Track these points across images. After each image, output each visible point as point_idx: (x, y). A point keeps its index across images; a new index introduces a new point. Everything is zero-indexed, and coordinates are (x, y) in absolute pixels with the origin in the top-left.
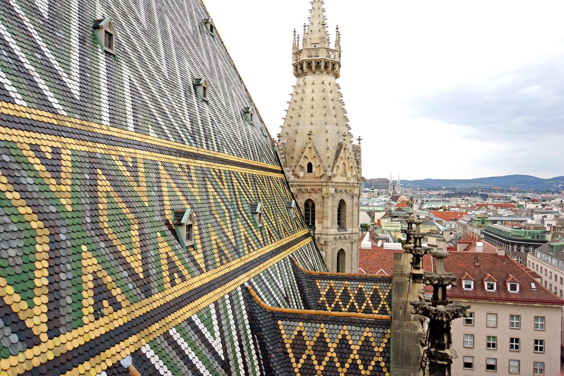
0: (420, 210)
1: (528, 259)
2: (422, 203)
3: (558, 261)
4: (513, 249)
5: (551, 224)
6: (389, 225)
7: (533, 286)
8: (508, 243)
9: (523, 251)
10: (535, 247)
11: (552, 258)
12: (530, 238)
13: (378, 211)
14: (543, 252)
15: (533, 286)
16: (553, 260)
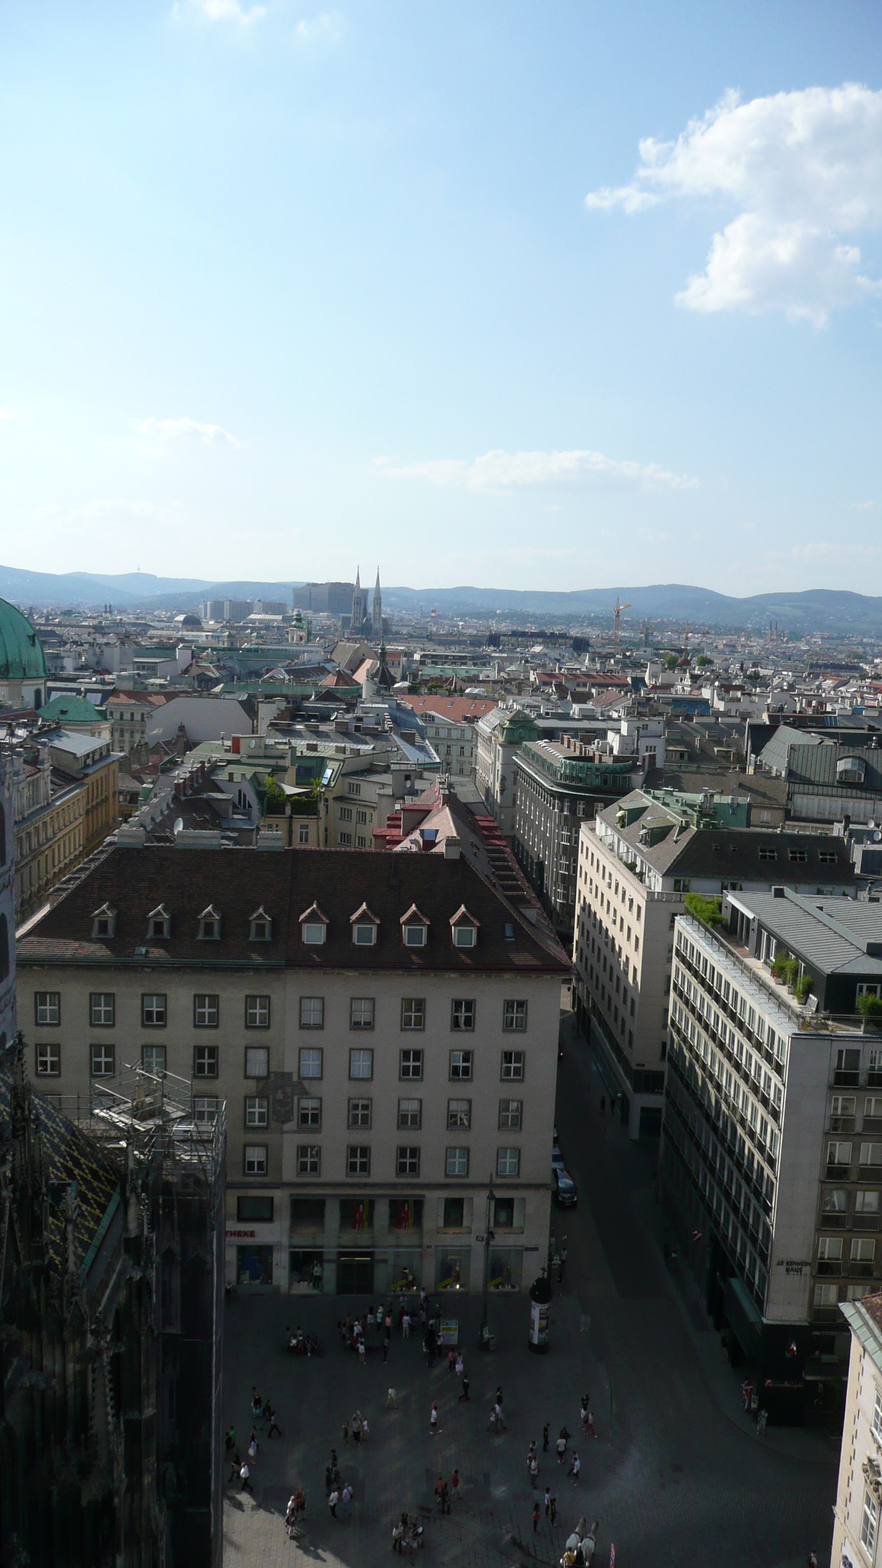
0: (379, 699)
1: (582, 837)
2: (422, 663)
3: (628, 848)
4: (562, 810)
5: (653, 745)
6: (261, 752)
7: (509, 932)
8: (553, 794)
9: (581, 815)
10: (607, 803)
11: (619, 840)
12: (597, 782)
13: (269, 697)
14: (609, 824)
15: (509, 932)
16: (621, 842)
